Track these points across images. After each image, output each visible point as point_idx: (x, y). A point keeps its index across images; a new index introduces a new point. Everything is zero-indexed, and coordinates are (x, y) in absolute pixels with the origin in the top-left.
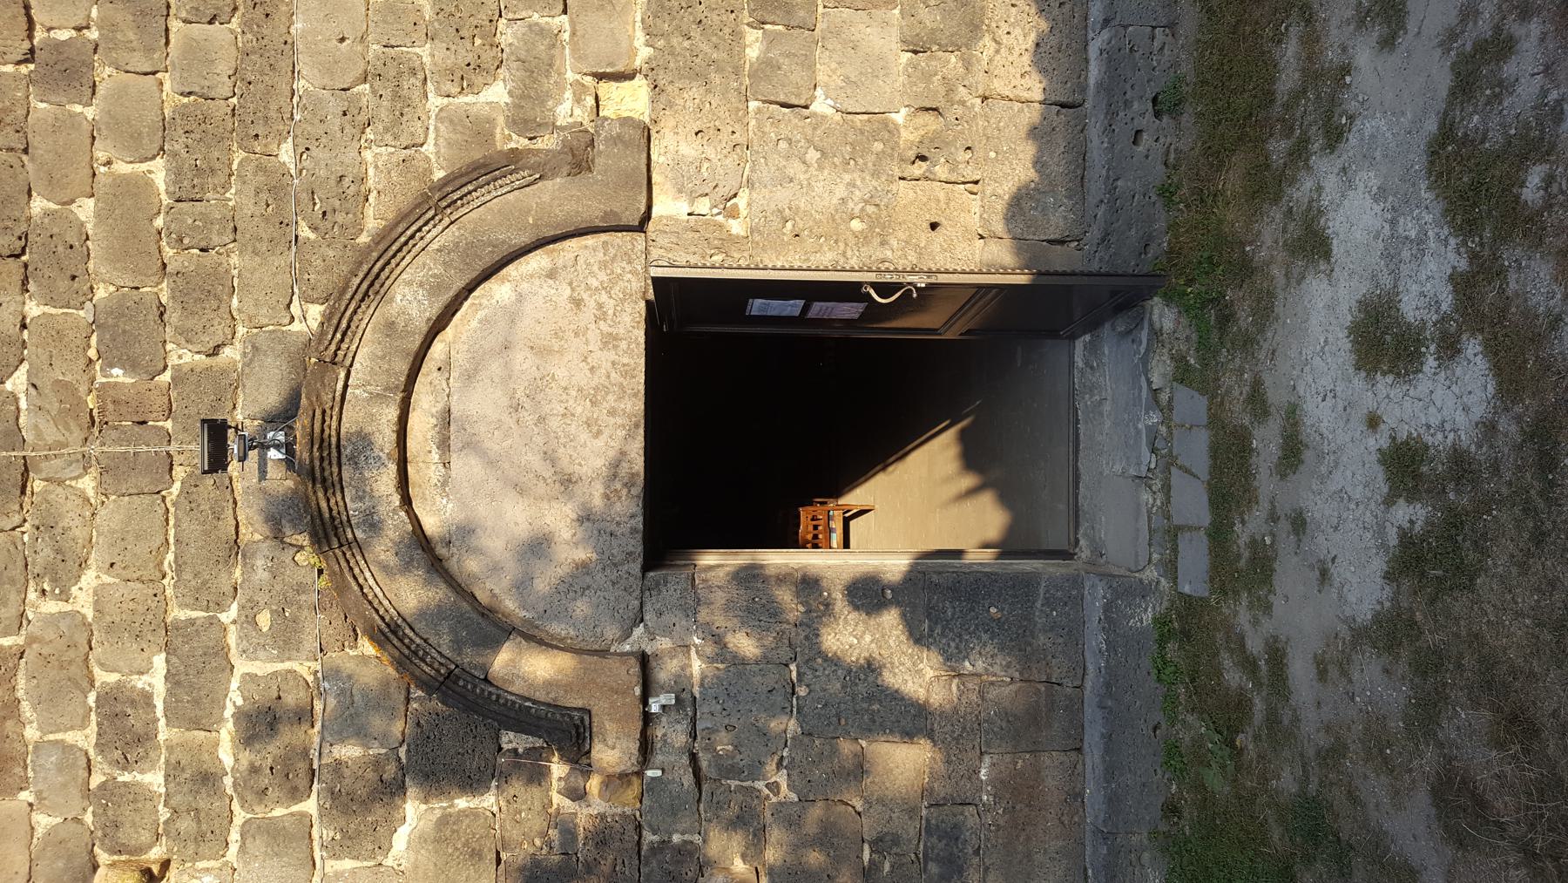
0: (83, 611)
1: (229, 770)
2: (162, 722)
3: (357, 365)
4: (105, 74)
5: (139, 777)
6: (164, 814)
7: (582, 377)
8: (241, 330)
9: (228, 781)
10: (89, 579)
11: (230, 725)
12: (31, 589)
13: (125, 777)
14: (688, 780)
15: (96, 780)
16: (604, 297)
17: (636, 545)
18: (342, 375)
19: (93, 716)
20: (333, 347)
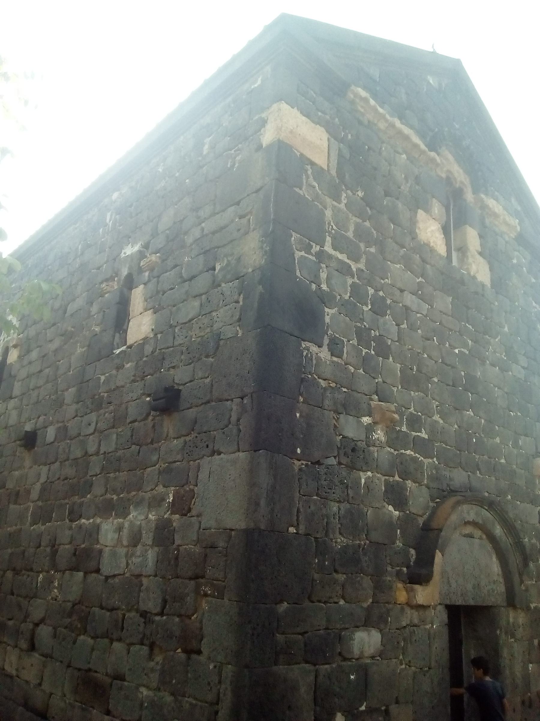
0: (434, 417)
1: (406, 452)
2: (416, 434)
3: (487, 513)
4: (515, 451)
5: (405, 423)
6: (398, 428)
7: (483, 583)
8: (482, 477)
9: (403, 451)
10: (441, 422)
11: (414, 455)
12: (439, 403)
13: (405, 420)
14: (404, 624)
15: (404, 409)
16: (496, 592)
17: (453, 603)
18: (487, 508)
19: (416, 413)
20: (495, 507)
